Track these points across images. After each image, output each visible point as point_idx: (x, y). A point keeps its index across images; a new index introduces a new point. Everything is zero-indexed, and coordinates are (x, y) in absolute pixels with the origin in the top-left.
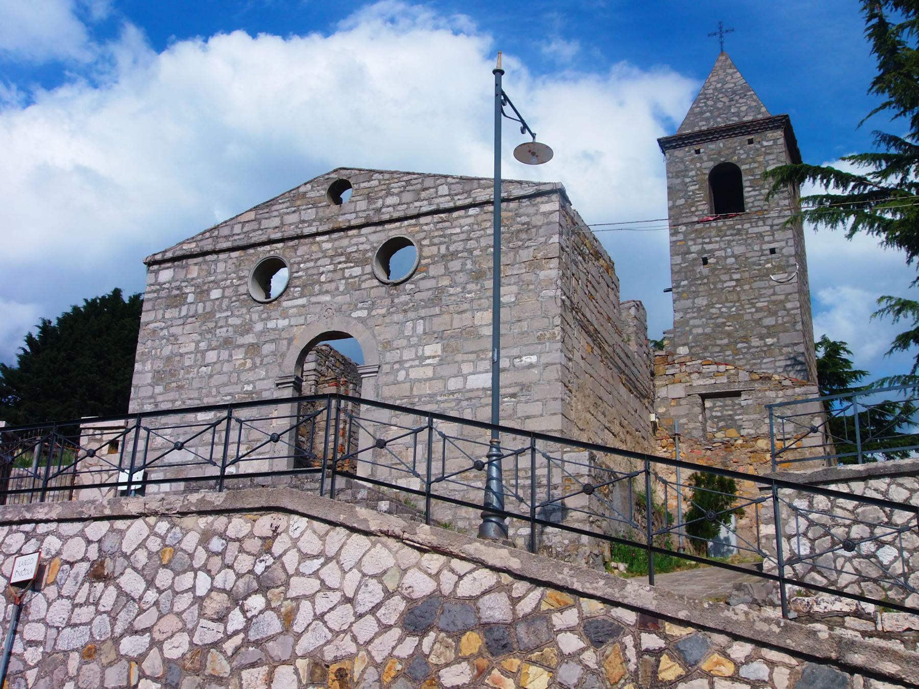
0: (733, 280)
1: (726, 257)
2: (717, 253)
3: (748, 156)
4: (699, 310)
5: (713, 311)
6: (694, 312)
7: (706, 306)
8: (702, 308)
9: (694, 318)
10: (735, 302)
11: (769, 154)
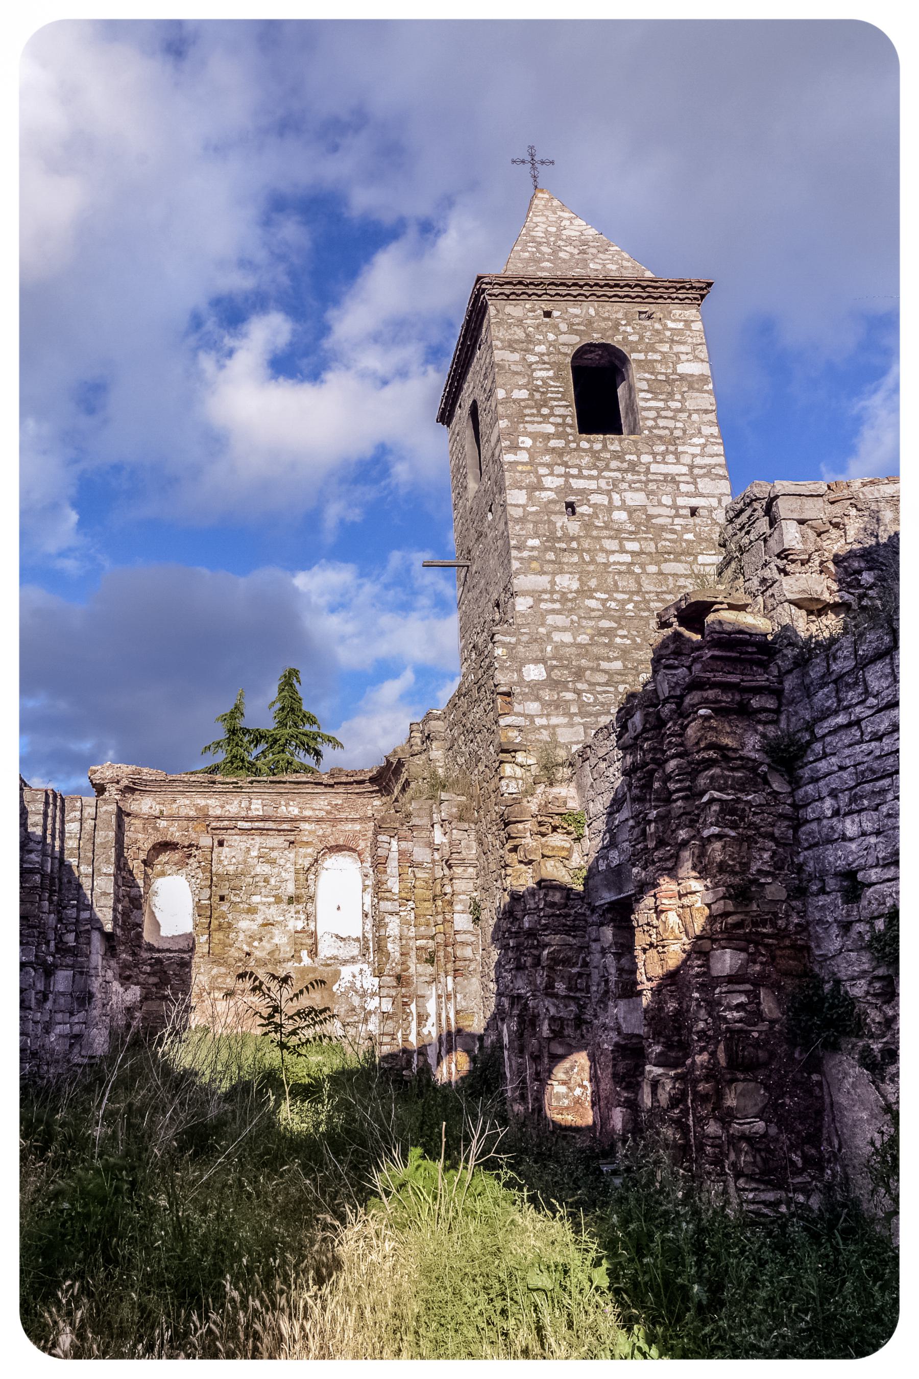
0: (627, 552)
1: (610, 508)
2: (595, 498)
3: (642, 338)
4: (564, 598)
5: (592, 603)
6: (553, 601)
7: (577, 592)
8: (570, 596)
9: (553, 611)
10: (633, 593)
11: (680, 343)
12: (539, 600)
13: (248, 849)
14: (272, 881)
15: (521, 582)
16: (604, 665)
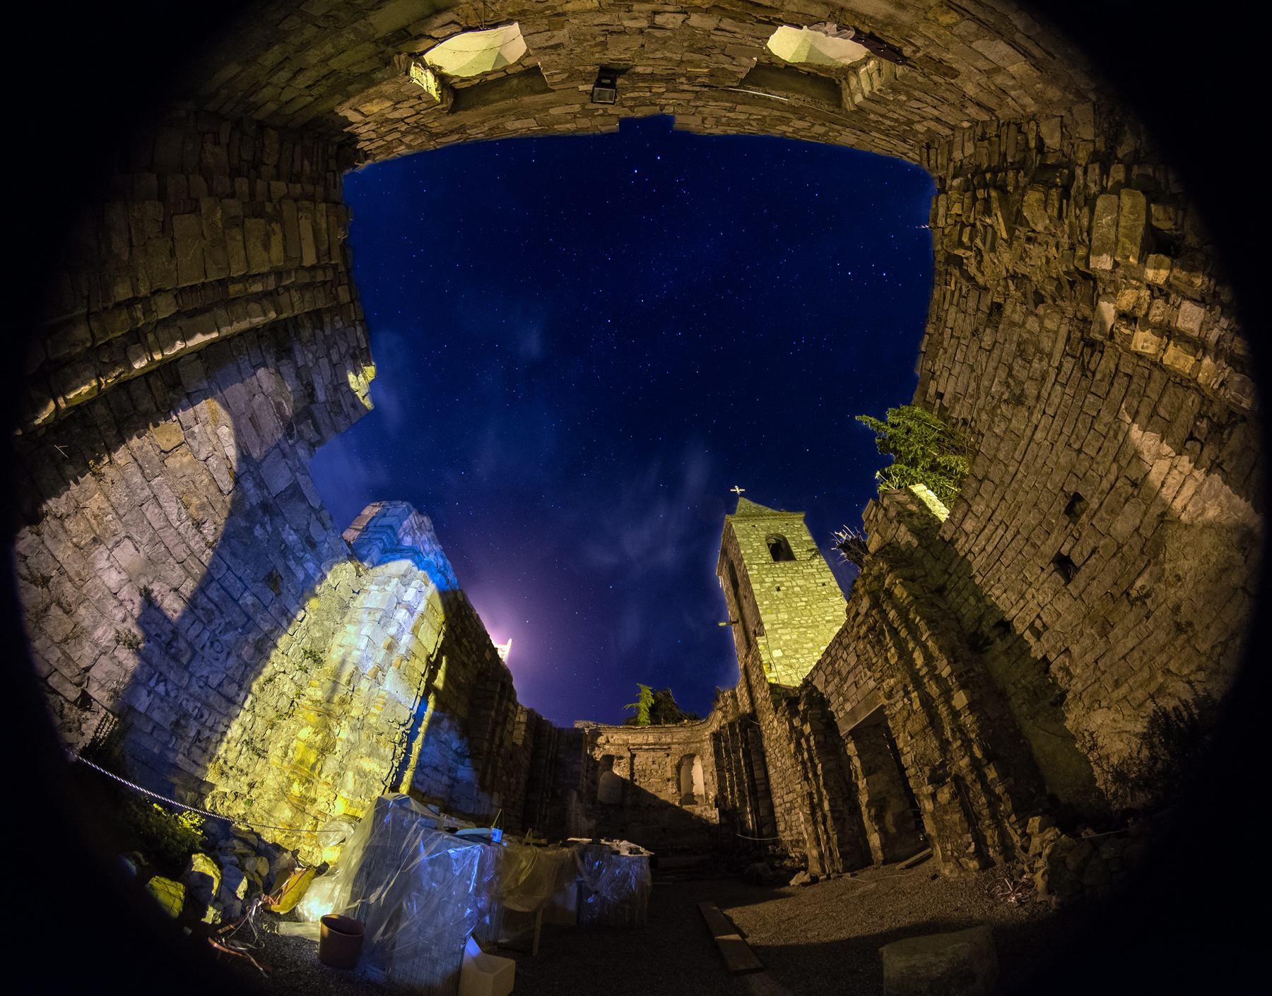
1: (793, 587)
2: (786, 584)
12: (773, 624)
15: (764, 618)
16: (805, 646)
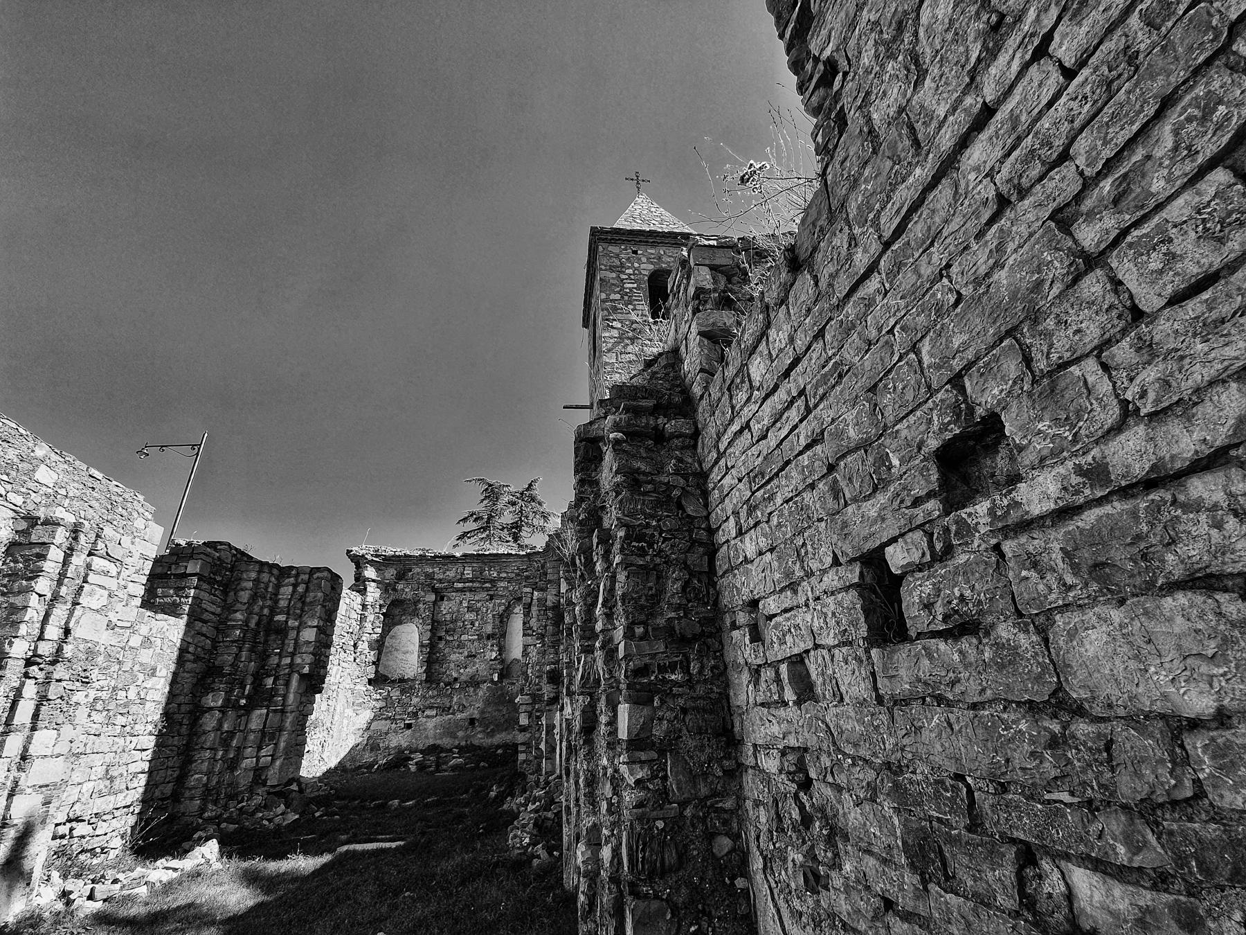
13: (461, 602)
14: (477, 624)
